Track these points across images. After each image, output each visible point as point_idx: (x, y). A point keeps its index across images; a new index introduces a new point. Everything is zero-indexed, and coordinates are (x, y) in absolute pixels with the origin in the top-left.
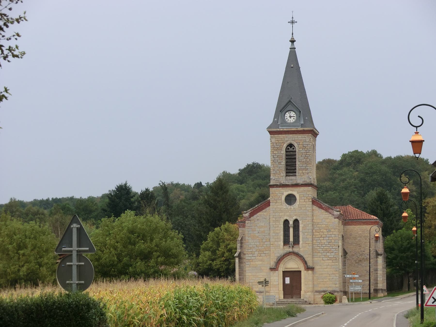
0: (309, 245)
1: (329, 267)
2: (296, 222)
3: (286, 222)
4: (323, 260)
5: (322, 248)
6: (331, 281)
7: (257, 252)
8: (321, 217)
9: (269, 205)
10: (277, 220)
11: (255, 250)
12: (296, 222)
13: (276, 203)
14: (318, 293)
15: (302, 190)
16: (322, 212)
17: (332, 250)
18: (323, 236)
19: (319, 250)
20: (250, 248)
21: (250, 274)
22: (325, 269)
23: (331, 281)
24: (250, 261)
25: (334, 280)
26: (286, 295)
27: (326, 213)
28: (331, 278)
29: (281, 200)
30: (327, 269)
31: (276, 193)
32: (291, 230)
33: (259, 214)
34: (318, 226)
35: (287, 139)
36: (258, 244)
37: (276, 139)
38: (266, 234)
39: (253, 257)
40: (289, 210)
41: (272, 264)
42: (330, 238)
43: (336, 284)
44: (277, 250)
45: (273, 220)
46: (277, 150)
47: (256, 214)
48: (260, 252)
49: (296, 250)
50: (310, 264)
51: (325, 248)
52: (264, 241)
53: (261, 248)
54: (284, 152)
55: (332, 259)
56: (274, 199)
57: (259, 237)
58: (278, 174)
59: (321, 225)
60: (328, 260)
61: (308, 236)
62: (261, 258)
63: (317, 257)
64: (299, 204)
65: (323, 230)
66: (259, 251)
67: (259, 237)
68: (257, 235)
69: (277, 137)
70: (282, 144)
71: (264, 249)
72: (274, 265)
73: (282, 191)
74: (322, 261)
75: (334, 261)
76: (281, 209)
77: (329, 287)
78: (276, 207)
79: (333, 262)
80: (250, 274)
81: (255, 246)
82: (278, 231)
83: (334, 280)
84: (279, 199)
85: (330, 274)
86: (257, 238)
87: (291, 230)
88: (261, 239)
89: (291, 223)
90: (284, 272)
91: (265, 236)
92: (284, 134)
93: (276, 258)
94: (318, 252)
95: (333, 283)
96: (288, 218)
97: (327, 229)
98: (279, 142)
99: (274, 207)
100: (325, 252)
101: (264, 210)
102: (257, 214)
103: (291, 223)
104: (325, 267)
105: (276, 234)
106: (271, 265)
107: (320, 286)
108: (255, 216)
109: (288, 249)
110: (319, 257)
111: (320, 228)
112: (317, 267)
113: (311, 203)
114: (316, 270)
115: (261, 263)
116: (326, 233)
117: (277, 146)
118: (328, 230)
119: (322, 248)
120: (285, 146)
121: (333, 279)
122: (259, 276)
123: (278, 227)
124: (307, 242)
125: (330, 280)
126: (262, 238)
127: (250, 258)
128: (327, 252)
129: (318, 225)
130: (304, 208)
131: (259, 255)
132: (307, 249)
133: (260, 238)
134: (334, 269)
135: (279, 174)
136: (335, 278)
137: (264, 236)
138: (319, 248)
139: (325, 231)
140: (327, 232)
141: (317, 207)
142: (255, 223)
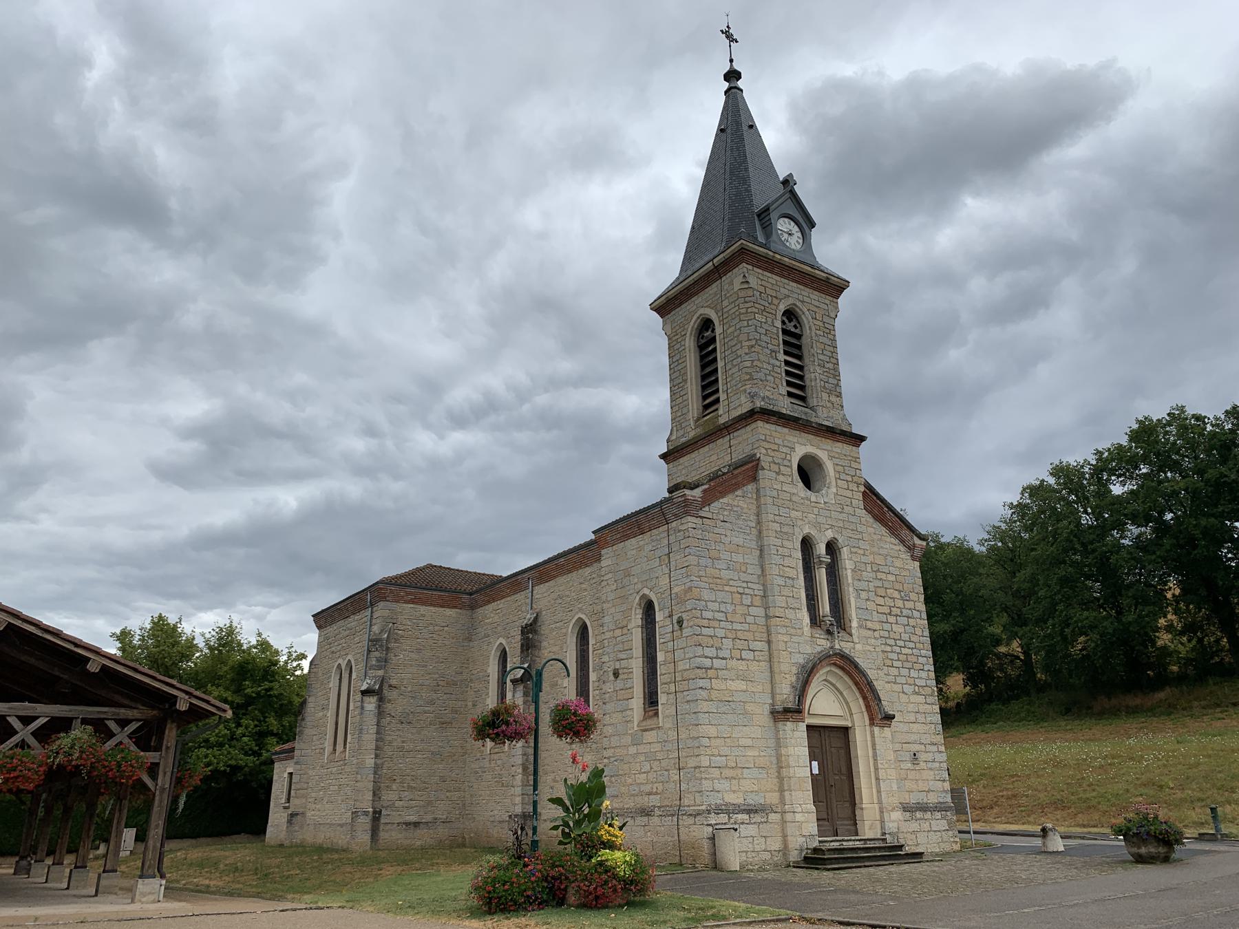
3: (807, 544)
7: (728, 643)
9: (754, 479)
10: (786, 533)
11: (721, 633)
13: (778, 473)
20: (705, 623)
21: (712, 731)
24: (711, 673)
29: (791, 467)
31: (777, 441)
33: (724, 500)
35: (786, 292)
36: (730, 608)
37: (760, 282)
38: (749, 578)
39: (717, 658)
40: (813, 504)
41: (785, 693)
44: (795, 639)
45: (776, 531)
46: (764, 313)
47: (718, 499)
48: (739, 644)
49: (842, 645)
52: (747, 601)
53: (736, 626)
54: (778, 324)
56: (770, 459)
57: (731, 583)
58: (772, 385)
62: (742, 665)
66: (733, 639)
67: (731, 583)
68: (725, 574)
69: (760, 276)
70: (775, 301)
71: (749, 631)
72: (791, 698)
73: (791, 438)
76: (794, 498)
78: (779, 487)
80: (712, 731)
82: (792, 573)
84: (786, 463)
86: (727, 588)
88: (738, 592)
91: (749, 585)
92: (777, 274)
93: (794, 670)
96: (813, 532)
98: (769, 291)
99: (775, 487)
101: (739, 492)
102: (721, 500)
105: (787, 580)
106: (778, 697)
108: (716, 505)
115: (742, 685)
117: (762, 302)
120: (782, 308)
122: (743, 742)
123: (791, 556)
126: (741, 590)
127: (708, 663)
131: (736, 654)
133: (735, 589)
135: (775, 386)
137: (745, 585)
142: (716, 530)
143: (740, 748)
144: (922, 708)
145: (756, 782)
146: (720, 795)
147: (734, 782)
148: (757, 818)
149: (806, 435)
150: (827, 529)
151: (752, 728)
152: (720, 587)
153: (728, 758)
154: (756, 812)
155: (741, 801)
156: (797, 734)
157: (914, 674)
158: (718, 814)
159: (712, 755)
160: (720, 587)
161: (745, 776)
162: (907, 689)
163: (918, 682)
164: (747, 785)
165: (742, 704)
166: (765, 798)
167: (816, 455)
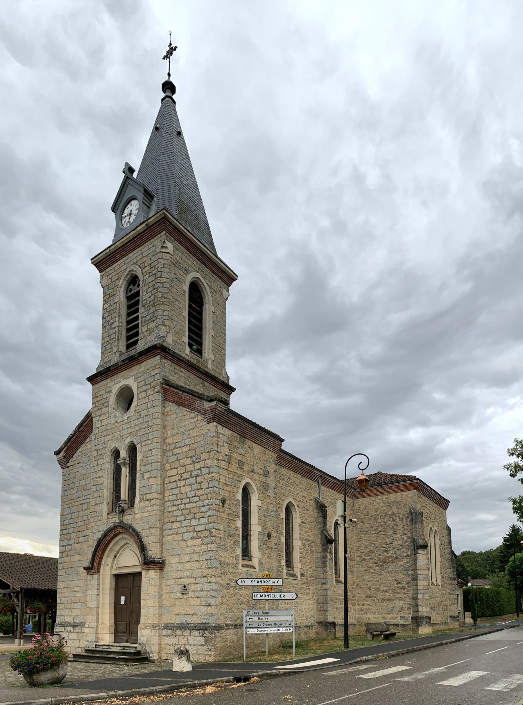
0: (153, 502)
1: (195, 557)
2: (133, 449)
3: (116, 453)
4: (183, 540)
5: (182, 507)
6: (198, 597)
7: (74, 535)
8: (181, 427)
12: (133, 449)
14: (170, 631)
15: (142, 369)
16: (184, 413)
17: (203, 509)
18: (185, 475)
19: (176, 513)
22: (185, 564)
23: (198, 597)
25: (205, 593)
26: (120, 634)
27: (192, 415)
28: (199, 587)
30: (192, 564)
32: (125, 471)
34: (175, 451)
42: (199, 479)
43: (209, 606)
50: (154, 553)
51: (188, 506)
55: (202, 536)
59: (180, 449)
60: (194, 538)
61: (150, 480)
63: (171, 535)
64: (138, 406)
65: (184, 460)
74: (182, 544)
75: (206, 541)
77: (193, 615)
79: (202, 544)
81: (71, 521)
83: (205, 593)
85: (195, 578)
87: (125, 471)
89: (123, 454)
90: (118, 577)
94: (173, 519)
95: (203, 603)
97: (191, 457)
100: (188, 517)
103: (123, 454)
104: (188, 558)
107: (176, 610)
109: (115, 520)
110: (176, 534)
111: (180, 456)
112: (171, 561)
113: (159, 396)
114: (167, 568)
116: (190, 468)
118: (194, 459)
119: (182, 507)
121: (202, 590)
124: (148, 497)
125: (197, 594)
128: (191, 516)
129: (176, 448)
130: (145, 412)
132: (147, 514)
134: (206, 562)
136: (207, 587)
138: (175, 508)
139: (189, 461)
140: (194, 463)
141: (174, 405)
143: (74, 593)
144: (197, 549)
145: (79, 610)
146: (63, 617)
147: (70, 610)
148: (77, 630)
149: (122, 373)
150: (127, 437)
151: (80, 581)
152: (73, 505)
153: (69, 598)
154: (76, 626)
155: (72, 621)
156: (92, 582)
157: (194, 522)
158: (60, 627)
159: (62, 597)
160: (73, 505)
161: (75, 608)
162: (187, 536)
163: (197, 528)
164: (76, 612)
165: (77, 568)
166: (83, 619)
167: (126, 384)
